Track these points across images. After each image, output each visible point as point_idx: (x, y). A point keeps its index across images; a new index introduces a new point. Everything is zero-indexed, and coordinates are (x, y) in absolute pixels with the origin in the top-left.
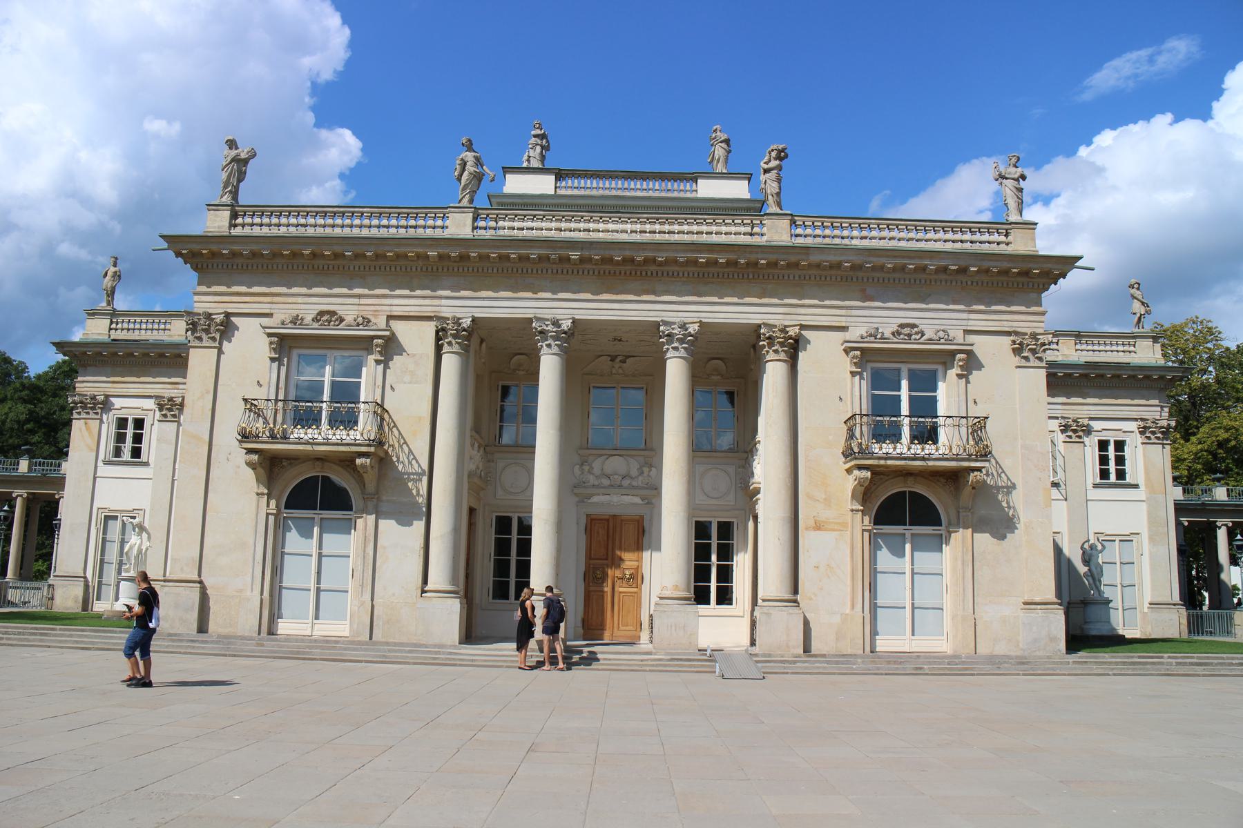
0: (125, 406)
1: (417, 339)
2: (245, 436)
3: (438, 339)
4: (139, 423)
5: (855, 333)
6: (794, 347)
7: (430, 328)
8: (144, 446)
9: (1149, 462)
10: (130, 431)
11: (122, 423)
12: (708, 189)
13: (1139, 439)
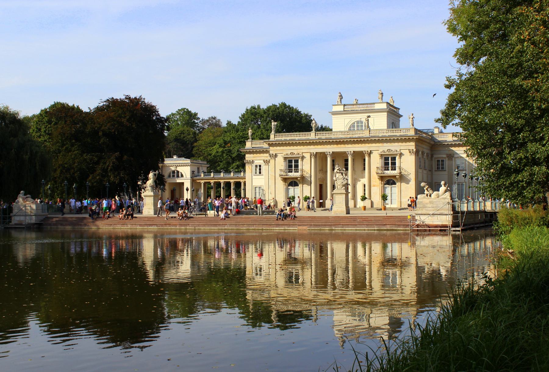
0: (257, 162)
1: (307, 156)
2: (280, 175)
4: (260, 166)
5: (379, 152)
6: (370, 154)
7: (309, 154)
11: (256, 166)
12: (377, 106)
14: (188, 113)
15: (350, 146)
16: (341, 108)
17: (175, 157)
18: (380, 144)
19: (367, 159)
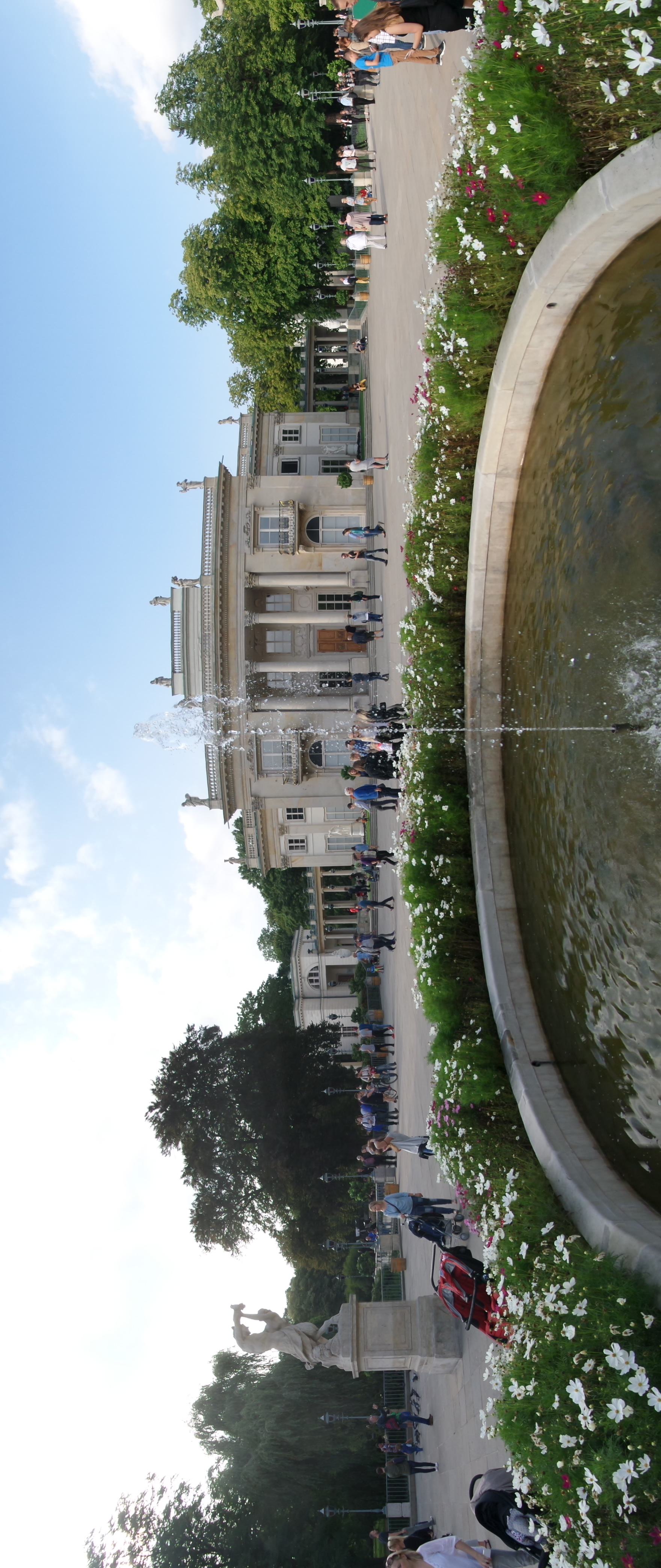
2: (297, 782)
3: (255, 711)
4: (291, 841)
8: (299, 838)
9: (291, 421)
10: (294, 844)
11: (291, 848)
12: (178, 606)
13: (282, 424)
14: (261, 939)
15: (232, 619)
16: (179, 678)
17: (290, 977)
18: (233, 551)
19: (263, 582)
